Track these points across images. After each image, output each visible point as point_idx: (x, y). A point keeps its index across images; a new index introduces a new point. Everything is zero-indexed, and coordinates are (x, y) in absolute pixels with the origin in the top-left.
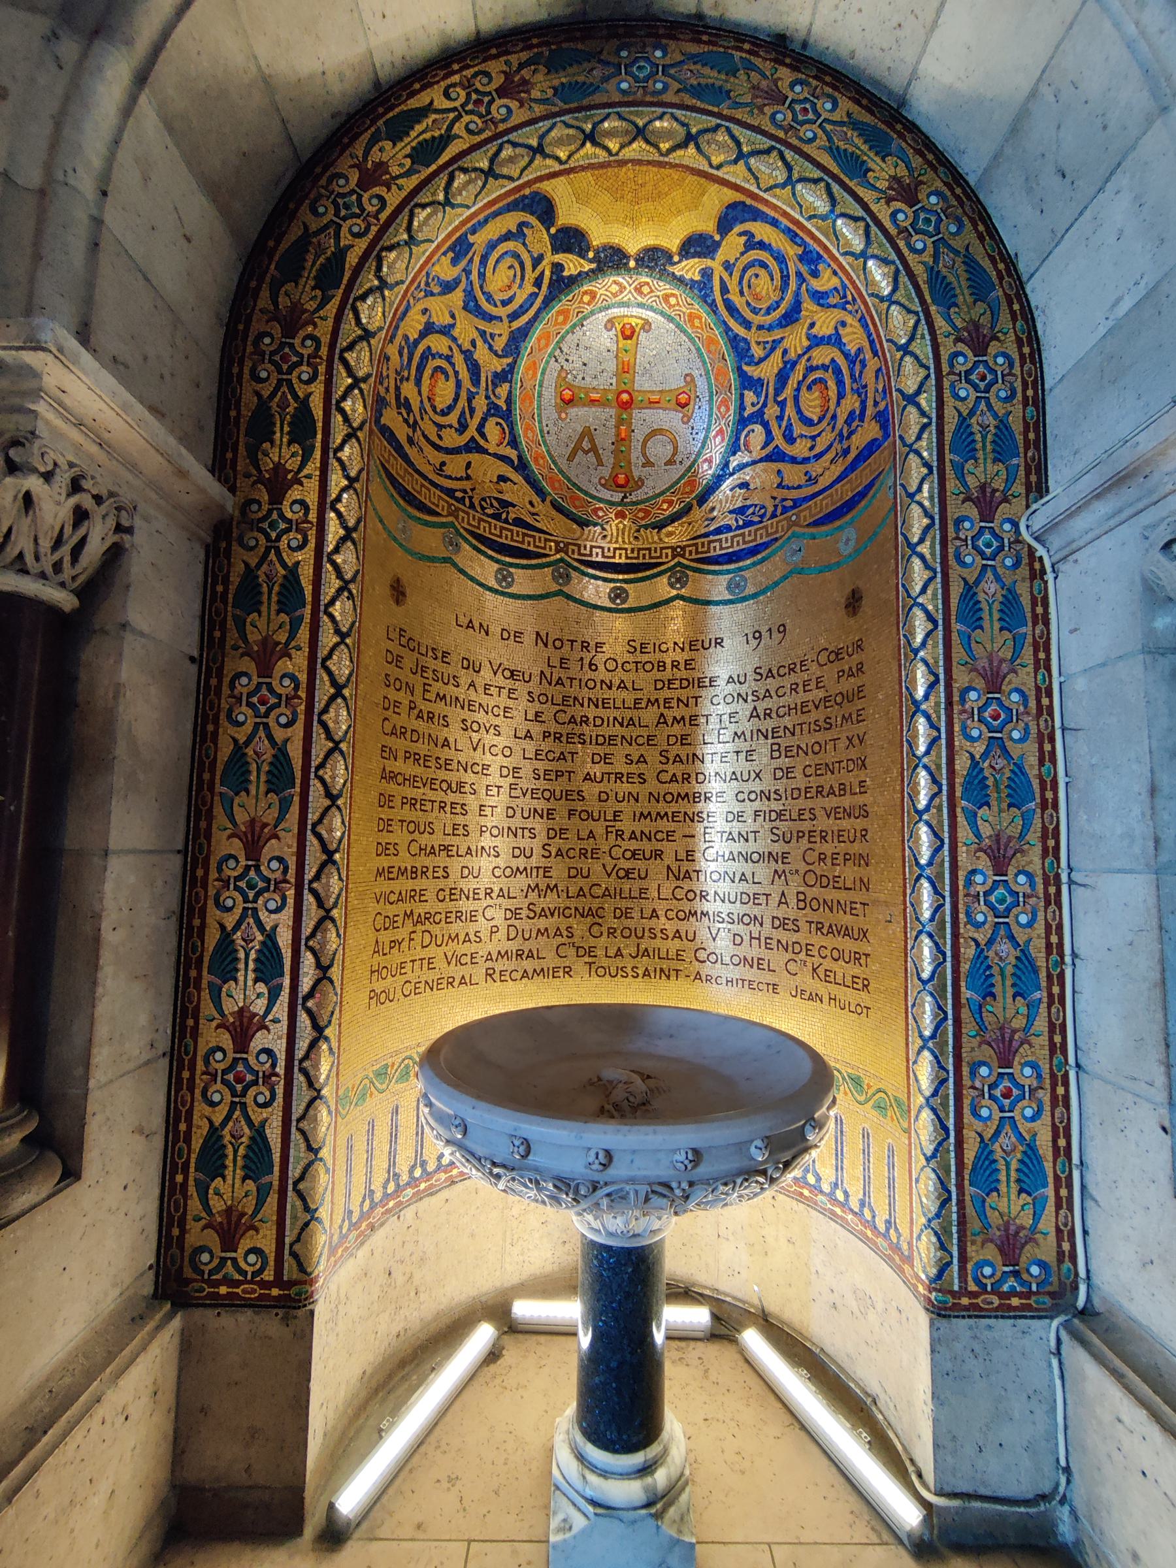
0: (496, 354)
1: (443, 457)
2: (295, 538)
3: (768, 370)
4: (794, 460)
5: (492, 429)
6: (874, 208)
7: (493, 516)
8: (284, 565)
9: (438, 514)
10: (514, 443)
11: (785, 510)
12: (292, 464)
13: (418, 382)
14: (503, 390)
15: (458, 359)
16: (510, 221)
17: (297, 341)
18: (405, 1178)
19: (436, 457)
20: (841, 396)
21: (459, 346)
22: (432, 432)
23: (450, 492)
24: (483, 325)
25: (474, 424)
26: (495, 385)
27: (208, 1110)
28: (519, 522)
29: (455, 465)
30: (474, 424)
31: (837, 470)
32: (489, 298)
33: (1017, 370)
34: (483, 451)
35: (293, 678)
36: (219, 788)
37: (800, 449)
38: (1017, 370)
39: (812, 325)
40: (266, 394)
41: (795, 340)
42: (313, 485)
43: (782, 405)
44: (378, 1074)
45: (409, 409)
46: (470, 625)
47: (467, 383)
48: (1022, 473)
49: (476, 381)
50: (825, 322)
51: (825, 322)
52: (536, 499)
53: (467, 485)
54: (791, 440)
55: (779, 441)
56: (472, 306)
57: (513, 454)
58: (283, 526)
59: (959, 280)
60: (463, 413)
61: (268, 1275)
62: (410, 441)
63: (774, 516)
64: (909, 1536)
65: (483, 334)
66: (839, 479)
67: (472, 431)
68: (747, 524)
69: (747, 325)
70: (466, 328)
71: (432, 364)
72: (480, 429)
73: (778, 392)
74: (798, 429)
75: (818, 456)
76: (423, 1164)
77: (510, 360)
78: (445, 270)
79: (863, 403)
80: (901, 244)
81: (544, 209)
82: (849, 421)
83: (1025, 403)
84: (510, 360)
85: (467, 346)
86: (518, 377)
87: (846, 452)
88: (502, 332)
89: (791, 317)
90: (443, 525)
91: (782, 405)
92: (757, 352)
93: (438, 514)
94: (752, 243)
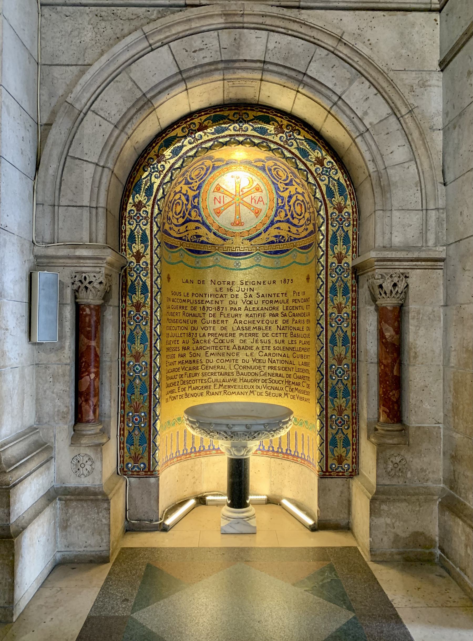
0: (194, 190)
1: (178, 228)
2: (143, 272)
3: (286, 195)
4: (295, 225)
5: (193, 214)
6: (310, 167)
7: (194, 242)
8: (142, 281)
9: (177, 247)
10: (200, 215)
11: (291, 240)
12: (142, 251)
13: (172, 210)
14: (196, 200)
15: (183, 198)
16: (200, 163)
17: (141, 212)
18: (174, 456)
19: (176, 229)
20: (305, 211)
21: (183, 194)
22: (175, 222)
23: (181, 238)
24: (189, 186)
25: (187, 213)
26: (194, 199)
27: (128, 428)
28: (202, 242)
29: (182, 229)
30: (187, 213)
31: (305, 233)
32: (192, 179)
33: (351, 217)
34: (191, 221)
35: (147, 313)
36: (127, 343)
37: (295, 221)
38: (351, 217)
39: (296, 189)
40: (133, 229)
41: (292, 189)
42: (148, 257)
43: (290, 206)
44: (169, 422)
45: (170, 219)
46: (187, 282)
47: (185, 202)
48: (351, 248)
49: (188, 200)
50: (300, 190)
51: (300, 190)
52: (208, 232)
53: (186, 234)
54: (293, 218)
55: (289, 216)
56: (187, 183)
57: (200, 219)
58: (140, 269)
59: (335, 189)
60: (184, 212)
61: (147, 470)
62: (170, 228)
63: (288, 241)
64: (310, 526)
65: (190, 188)
66: (306, 237)
67: (187, 215)
68: (280, 242)
69: (278, 181)
70: (185, 188)
71: (175, 203)
72: (190, 214)
73: (289, 202)
74: (295, 215)
75: (302, 226)
76: (179, 451)
77: (198, 191)
78: (181, 179)
79: (311, 217)
80: (318, 179)
81: (210, 158)
82: (308, 220)
83: (353, 226)
84: (198, 191)
85: (185, 192)
86: (201, 194)
87: (307, 229)
88: (195, 185)
89: (290, 184)
90: (179, 250)
91: (290, 206)
92: (282, 189)
93: (177, 247)
94: (276, 164)
